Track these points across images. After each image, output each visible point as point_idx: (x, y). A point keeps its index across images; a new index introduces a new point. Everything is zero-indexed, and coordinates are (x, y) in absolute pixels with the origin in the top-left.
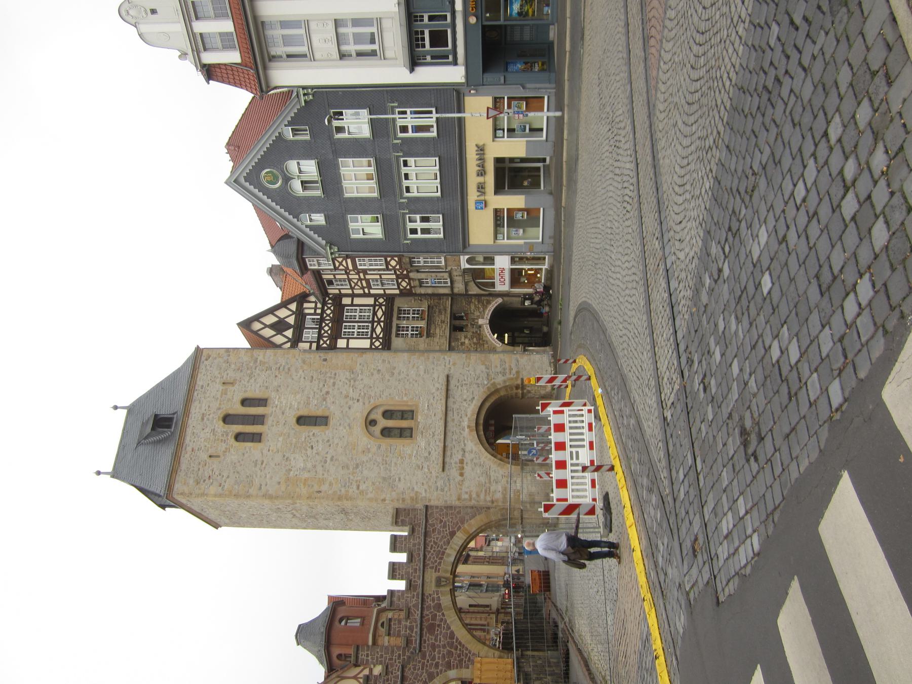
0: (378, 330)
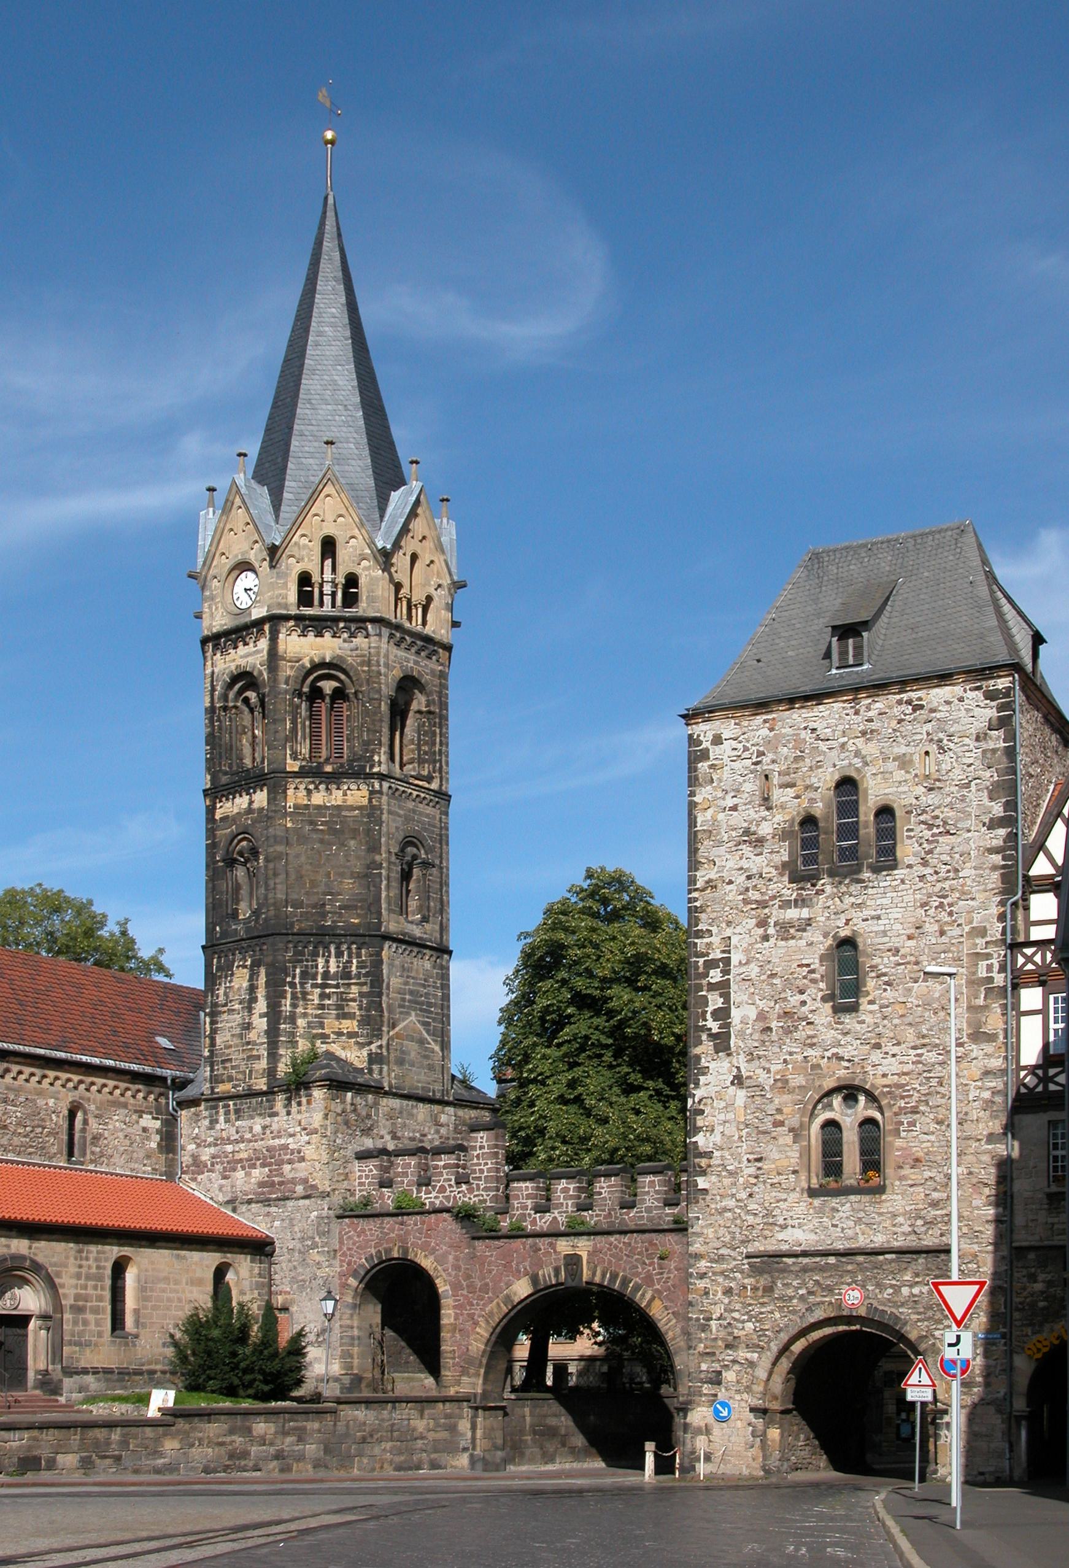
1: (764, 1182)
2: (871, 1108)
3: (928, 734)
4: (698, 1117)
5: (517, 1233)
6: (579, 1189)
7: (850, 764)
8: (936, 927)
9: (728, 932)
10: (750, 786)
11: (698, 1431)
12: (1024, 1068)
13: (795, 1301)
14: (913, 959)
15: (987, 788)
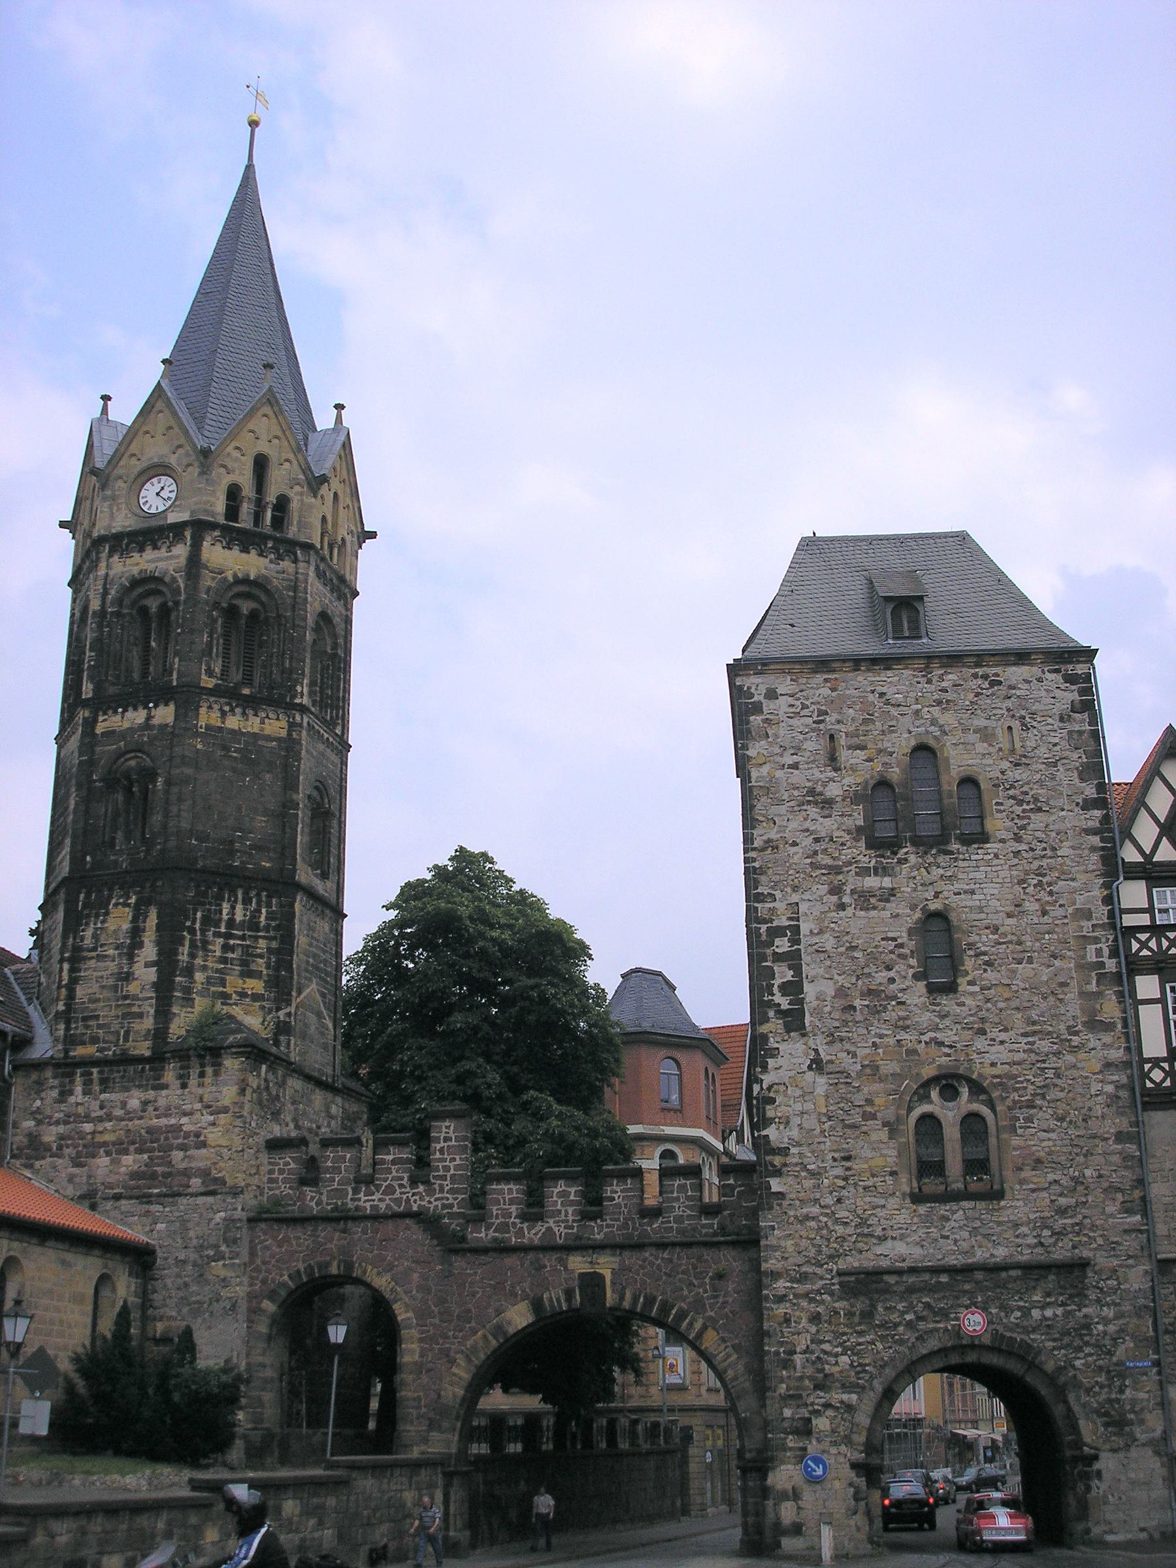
1: (855, 1184)
2: (977, 1101)
3: (1008, 710)
4: (768, 1107)
6: (583, 1194)
7: (927, 732)
8: (1037, 906)
9: (795, 898)
11: (784, 1496)
12: (1149, 1060)
13: (901, 1329)
14: (1014, 938)
15: (1077, 769)
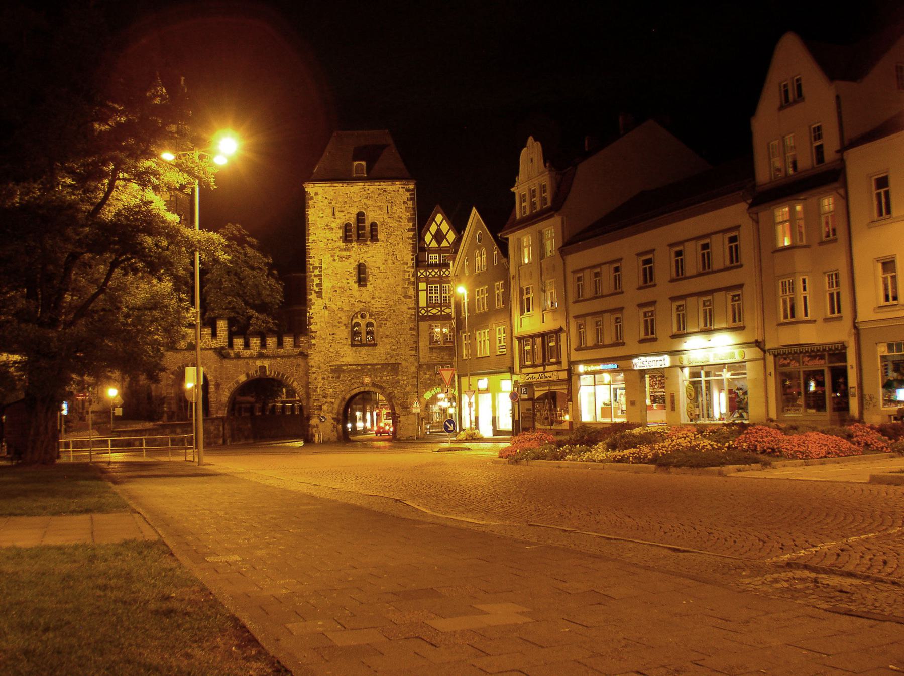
0: (434, 311)
5: (238, 357)
10: (329, 211)
11: (314, 427)
